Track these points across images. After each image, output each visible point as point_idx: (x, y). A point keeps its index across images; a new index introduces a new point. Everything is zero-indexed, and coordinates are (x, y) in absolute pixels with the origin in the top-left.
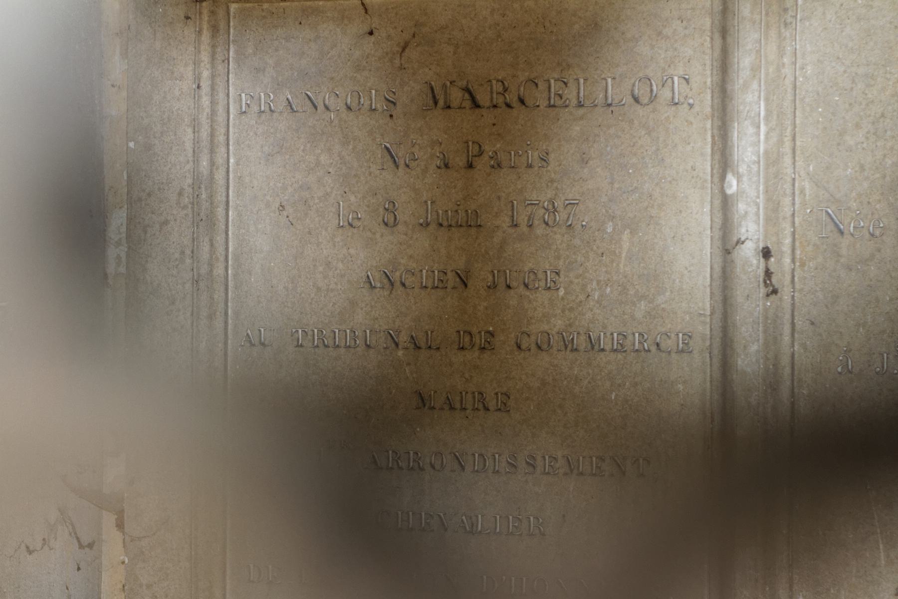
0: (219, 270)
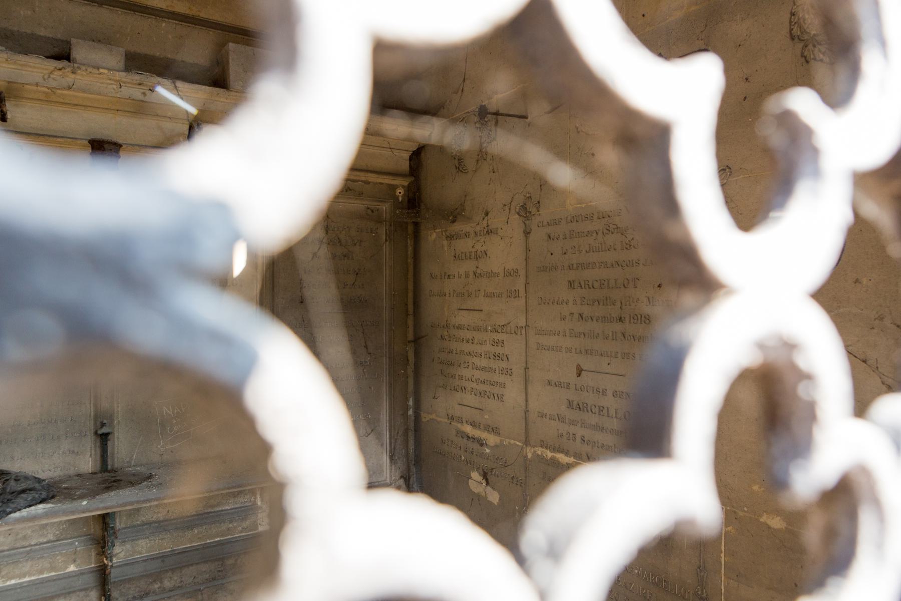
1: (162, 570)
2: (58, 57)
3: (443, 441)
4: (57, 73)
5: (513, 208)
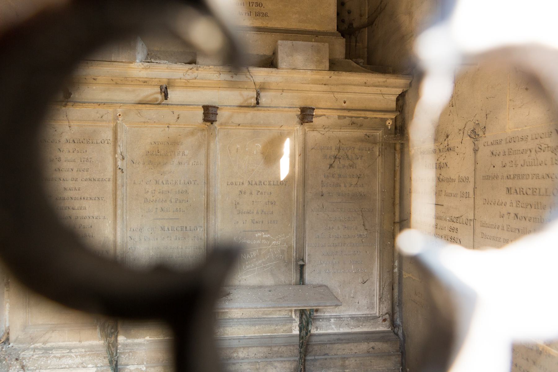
1: (238, 346)
2: (190, 63)
3: (416, 293)
4: (190, 71)
5: (465, 132)
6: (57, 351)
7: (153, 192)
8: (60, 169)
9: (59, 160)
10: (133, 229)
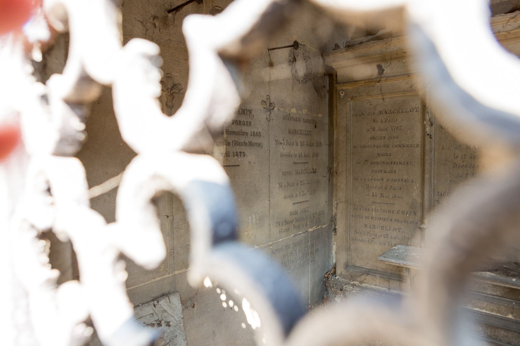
0: (350, 138)
6: (370, 291)
7: (463, 157)
8: (375, 137)
9: (374, 130)
10: (441, 194)
